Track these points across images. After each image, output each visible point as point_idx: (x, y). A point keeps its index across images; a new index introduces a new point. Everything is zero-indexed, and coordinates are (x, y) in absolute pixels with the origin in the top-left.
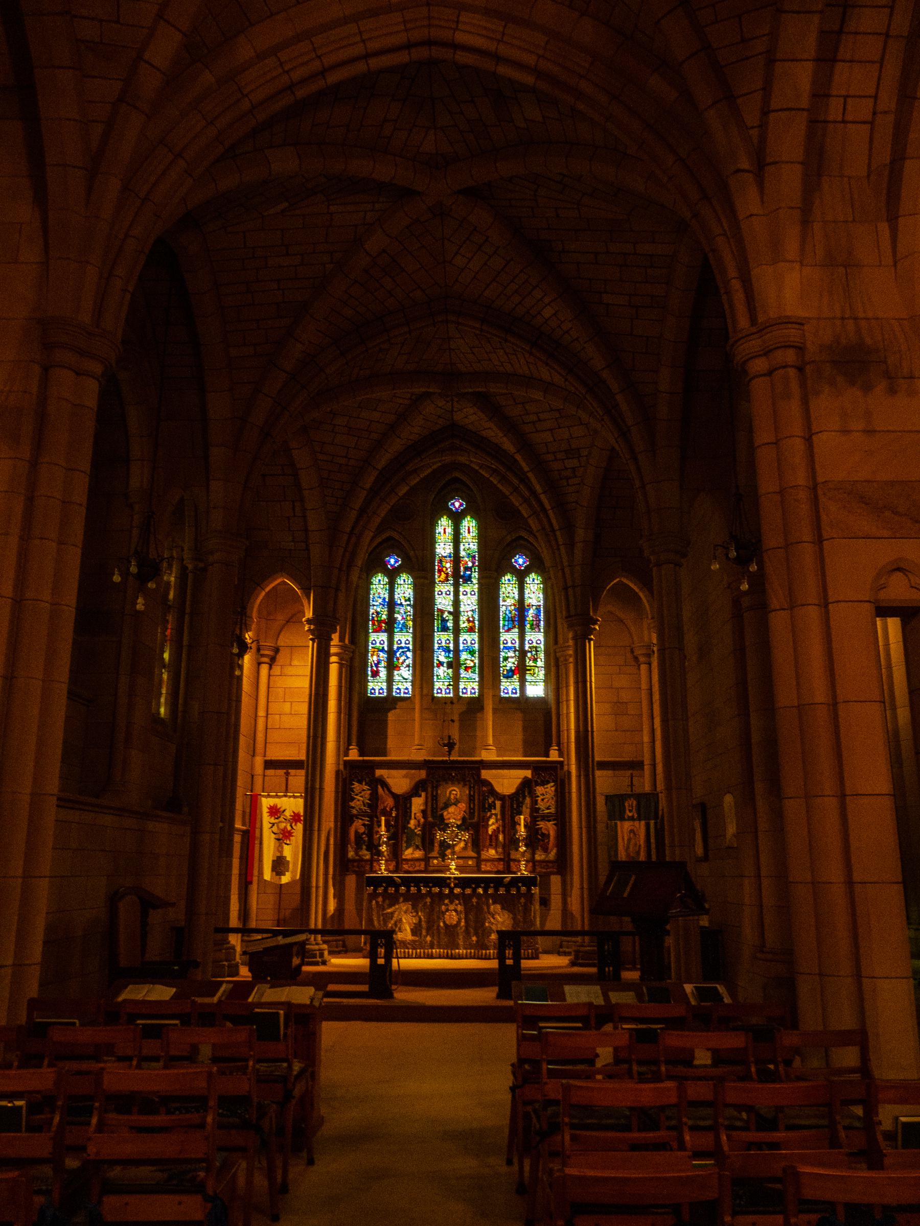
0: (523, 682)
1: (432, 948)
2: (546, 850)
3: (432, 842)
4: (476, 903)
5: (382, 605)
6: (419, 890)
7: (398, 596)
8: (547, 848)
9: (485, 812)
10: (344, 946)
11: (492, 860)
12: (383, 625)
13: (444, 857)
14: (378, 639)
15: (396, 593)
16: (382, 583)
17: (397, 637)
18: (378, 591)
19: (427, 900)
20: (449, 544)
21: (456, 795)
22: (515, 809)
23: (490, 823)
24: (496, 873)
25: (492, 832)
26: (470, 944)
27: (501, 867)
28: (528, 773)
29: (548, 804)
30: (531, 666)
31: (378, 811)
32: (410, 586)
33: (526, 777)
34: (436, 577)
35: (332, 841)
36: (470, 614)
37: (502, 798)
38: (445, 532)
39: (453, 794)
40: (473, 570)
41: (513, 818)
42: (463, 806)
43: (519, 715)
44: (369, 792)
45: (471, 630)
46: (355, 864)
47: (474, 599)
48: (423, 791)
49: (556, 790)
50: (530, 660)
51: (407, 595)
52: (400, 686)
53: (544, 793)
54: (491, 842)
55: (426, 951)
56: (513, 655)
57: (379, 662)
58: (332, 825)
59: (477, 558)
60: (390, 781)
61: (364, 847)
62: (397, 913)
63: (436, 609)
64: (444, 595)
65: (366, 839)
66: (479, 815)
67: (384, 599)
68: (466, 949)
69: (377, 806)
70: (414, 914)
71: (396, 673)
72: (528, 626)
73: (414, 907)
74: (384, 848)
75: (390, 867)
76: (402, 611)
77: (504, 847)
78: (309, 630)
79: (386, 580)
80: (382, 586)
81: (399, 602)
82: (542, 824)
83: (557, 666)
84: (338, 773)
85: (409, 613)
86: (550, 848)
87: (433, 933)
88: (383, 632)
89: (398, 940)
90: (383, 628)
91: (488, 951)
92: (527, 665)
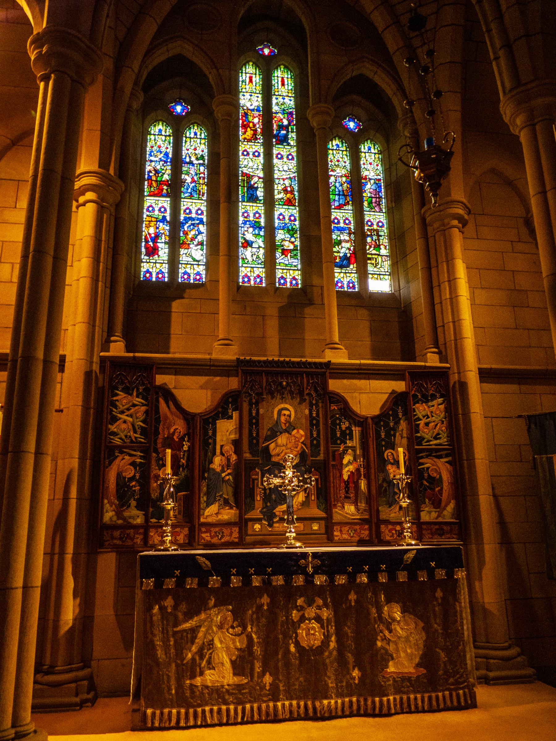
0: (363, 275)
1: (276, 699)
2: (437, 504)
3: (251, 495)
4: (356, 601)
5: (164, 161)
6: (247, 581)
7: (186, 152)
8: (441, 500)
9: (337, 444)
10: (92, 687)
11: (351, 524)
12: (165, 187)
13: (272, 520)
15: (184, 148)
16: (163, 133)
17: (185, 204)
18: (158, 144)
19: (263, 601)
20: (256, 95)
21: (290, 416)
22: (383, 440)
23: (345, 461)
24: (361, 543)
25: (349, 476)
26: (349, 685)
27: (365, 534)
28: (400, 386)
29: (436, 431)
30: (372, 254)
31: (160, 441)
32: (203, 141)
33: (393, 392)
34: (240, 133)
35: (74, 492)
36: (287, 183)
37: (362, 422)
38: (251, 81)
39: (285, 415)
40: (290, 130)
41: (380, 454)
42: (300, 433)
43: (363, 313)
44: (143, 408)
45: (289, 203)
46: (117, 534)
47: (292, 165)
48: (234, 410)
49: (447, 410)
50: (370, 247)
51: (199, 152)
52: (188, 270)
53: (429, 414)
54: (347, 492)
55: (264, 705)
56: (347, 238)
57: (157, 236)
58: (75, 463)
59: (294, 116)
60: (178, 393)
61: (133, 503)
62: (203, 629)
63: (240, 172)
64: (251, 156)
65: (138, 488)
66: (327, 449)
67: (166, 154)
68: (340, 695)
69: (157, 433)
70: (238, 630)
71: (182, 251)
72: (366, 204)
73: (238, 614)
74: (169, 505)
75: (178, 538)
76: (192, 172)
77: (369, 500)
78: (39, 57)
79: (169, 131)
80: (163, 138)
81: (188, 160)
82: (428, 463)
83: (425, 237)
84: (88, 375)
85: (202, 175)
86: (443, 504)
87: (276, 668)
88: (163, 196)
89: (207, 687)
90: (165, 191)
91: (385, 699)
92: (368, 252)
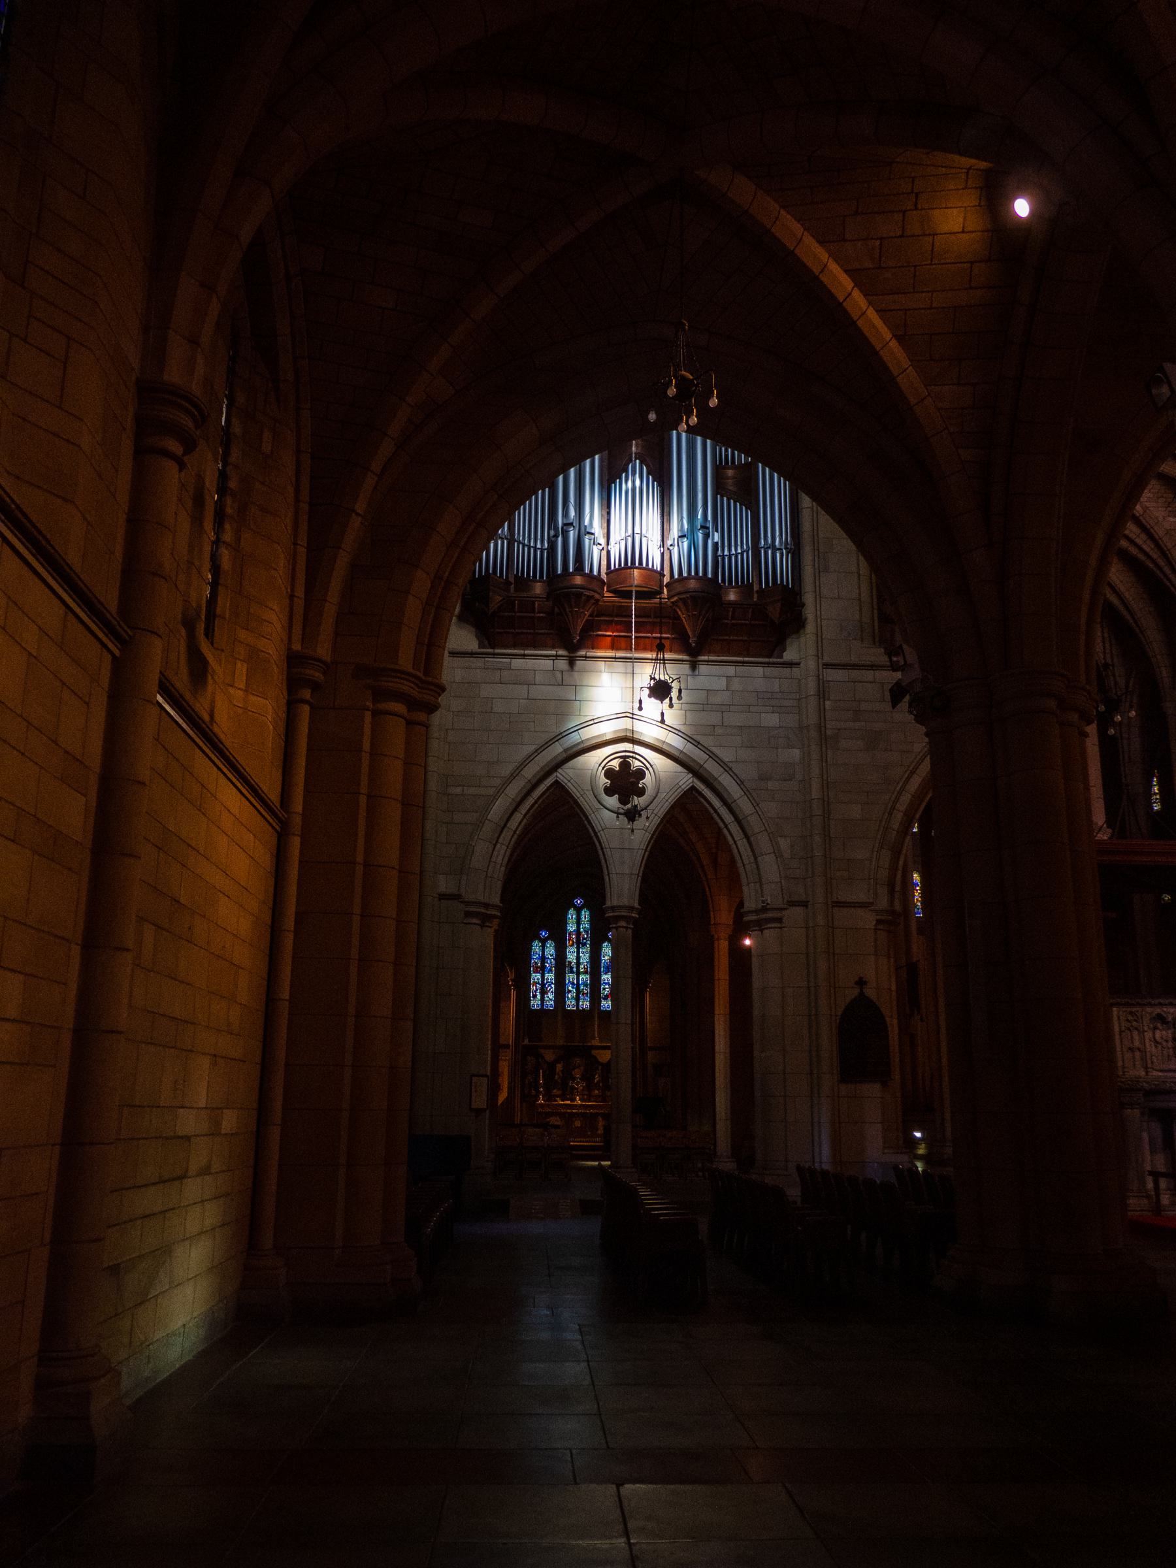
14: (536, 977)
37: (601, 1064)
45: (586, 973)
57: (537, 990)
67: (539, 955)
